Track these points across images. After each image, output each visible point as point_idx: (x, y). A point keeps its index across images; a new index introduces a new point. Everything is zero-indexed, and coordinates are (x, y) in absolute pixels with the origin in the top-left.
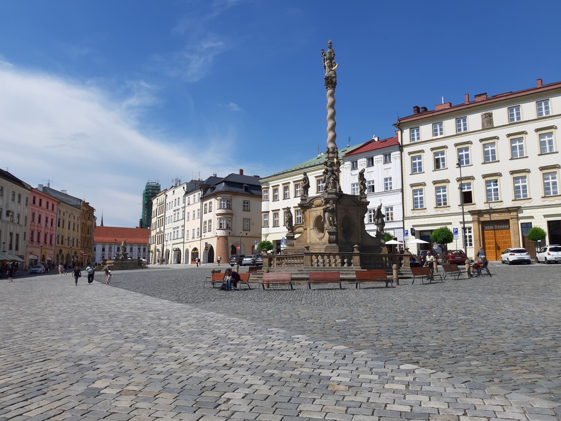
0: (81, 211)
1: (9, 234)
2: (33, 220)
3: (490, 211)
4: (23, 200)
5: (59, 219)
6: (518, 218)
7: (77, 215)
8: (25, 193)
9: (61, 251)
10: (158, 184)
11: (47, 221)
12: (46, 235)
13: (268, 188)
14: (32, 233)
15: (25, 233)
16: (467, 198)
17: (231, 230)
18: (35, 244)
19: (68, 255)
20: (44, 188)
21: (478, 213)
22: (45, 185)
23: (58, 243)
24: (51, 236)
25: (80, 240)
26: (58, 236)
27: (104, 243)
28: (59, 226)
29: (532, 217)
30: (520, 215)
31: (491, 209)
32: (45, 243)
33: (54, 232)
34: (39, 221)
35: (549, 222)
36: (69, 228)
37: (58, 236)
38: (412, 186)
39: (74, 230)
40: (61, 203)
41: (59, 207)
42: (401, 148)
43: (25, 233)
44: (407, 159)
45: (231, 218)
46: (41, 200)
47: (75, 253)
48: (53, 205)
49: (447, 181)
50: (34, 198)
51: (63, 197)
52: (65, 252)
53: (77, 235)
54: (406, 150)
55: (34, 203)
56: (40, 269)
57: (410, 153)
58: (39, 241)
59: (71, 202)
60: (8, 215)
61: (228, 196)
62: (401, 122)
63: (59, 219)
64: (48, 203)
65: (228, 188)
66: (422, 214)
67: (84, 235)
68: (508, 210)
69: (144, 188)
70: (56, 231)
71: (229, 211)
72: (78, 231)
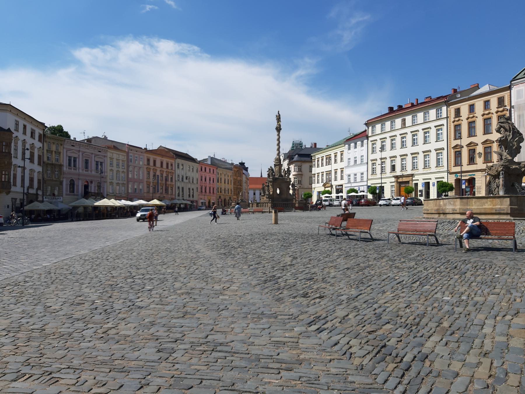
0: (233, 172)
1: (188, 189)
2: (202, 180)
3: (402, 176)
4: (195, 170)
5: (218, 178)
6: (412, 180)
7: (230, 174)
8: (196, 166)
9: (220, 197)
10: (301, 142)
11: (210, 180)
12: (210, 188)
13: (315, 159)
14: (202, 188)
15: (197, 188)
16: (393, 168)
17: (302, 184)
18: (203, 194)
19: (225, 200)
20: (212, 159)
21: (397, 177)
22: (212, 156)
23: (218, 192)
24: (213, 189)
25: (233, 190)
26: (218, 188)
27: (254, 190)
28: (218, 182)
29: (418, 180)
30: (414, 179)
31: (403, 175)
32: (210, 192)
33: (215, 186)
34: (205, 180)
35: (438, 182)
36: (225, 183)
37: (218, 188)
38: (372, 160)
39: (228, 184)
40: (219, 168)
41: (218, 171)
42: (367, 137)
43: (197, 188)
44: (370, 144)
45: (302, 177)
46: (205, 168)
47: (230, 198)
48: (213, 170)
49: (407, 155)
50: (202, 167)
51: (222, 163)
52: (222, 197)
53: (231, 186)
54: (370, 139)
55: (201, 170)
56: (203, 208)
57: (371, 141)
58: (206, 192)
59: (226, 166)
60: (186, 179)
61: (299, 163)
62: (369, 122)
63: (218, 178)
64: (210, 169)
65: (300, 159)
66: (375, 177)
67: (236, 186)
68: (408, 176)
69: (291, 145)
70: (216, 185)
71: (300, 173)
72: (231, 184)
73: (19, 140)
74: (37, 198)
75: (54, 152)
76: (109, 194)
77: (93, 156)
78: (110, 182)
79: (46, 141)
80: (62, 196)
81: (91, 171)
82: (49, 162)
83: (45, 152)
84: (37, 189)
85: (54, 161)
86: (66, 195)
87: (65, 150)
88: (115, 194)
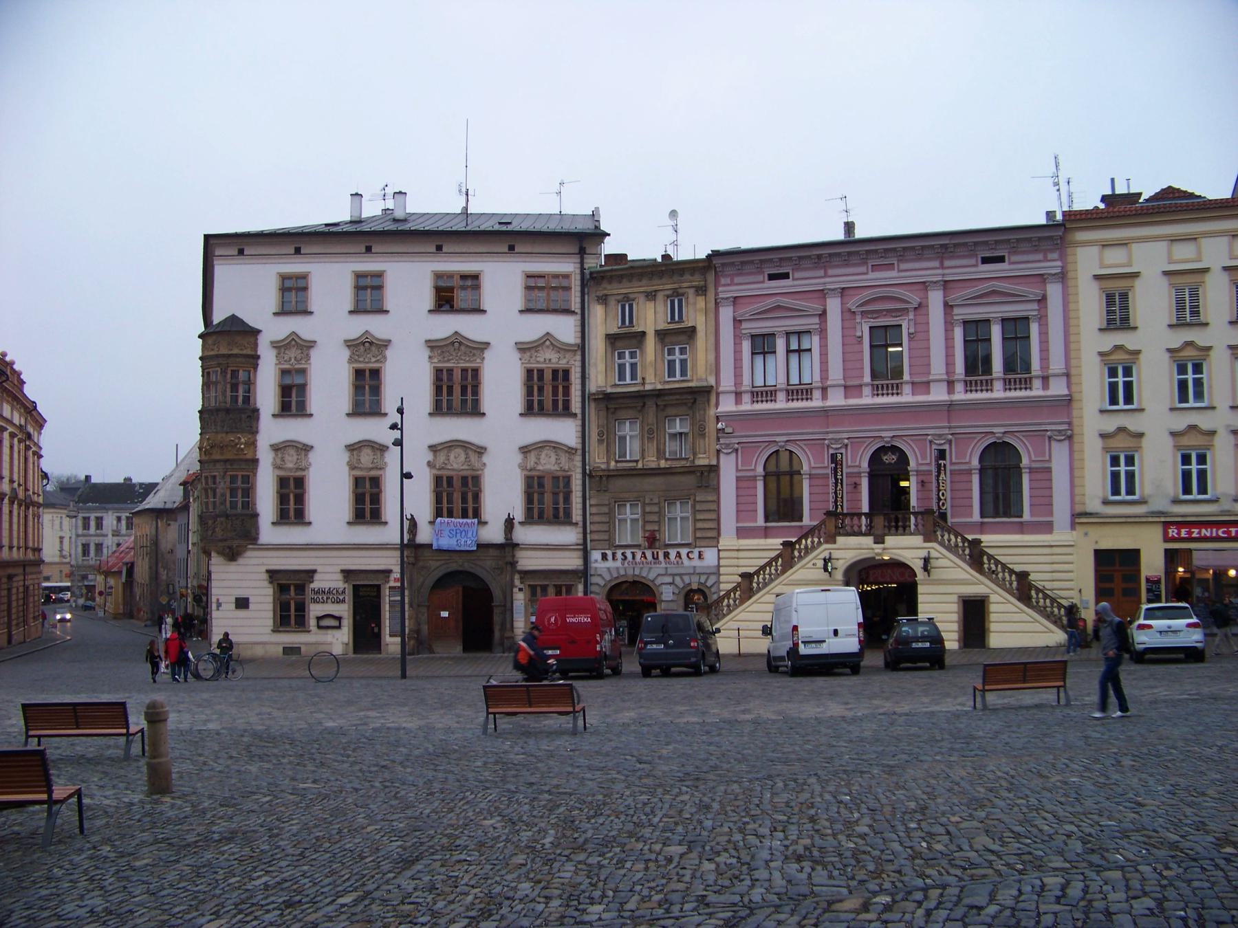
73: (311, 344)
74: (513, 564)
75: (650, 343)
76: (1094, 505)
77: (936, 299)
78: (1103, 436)
79: (604, 300)
80: (713, 538)
81: (923, 386)
82: (629, 386)
83: (597, 345)
84: (509, 523)
85: (650, 378)
86: (742, 533)
87: (726, 313)
88: (1160, 503)
